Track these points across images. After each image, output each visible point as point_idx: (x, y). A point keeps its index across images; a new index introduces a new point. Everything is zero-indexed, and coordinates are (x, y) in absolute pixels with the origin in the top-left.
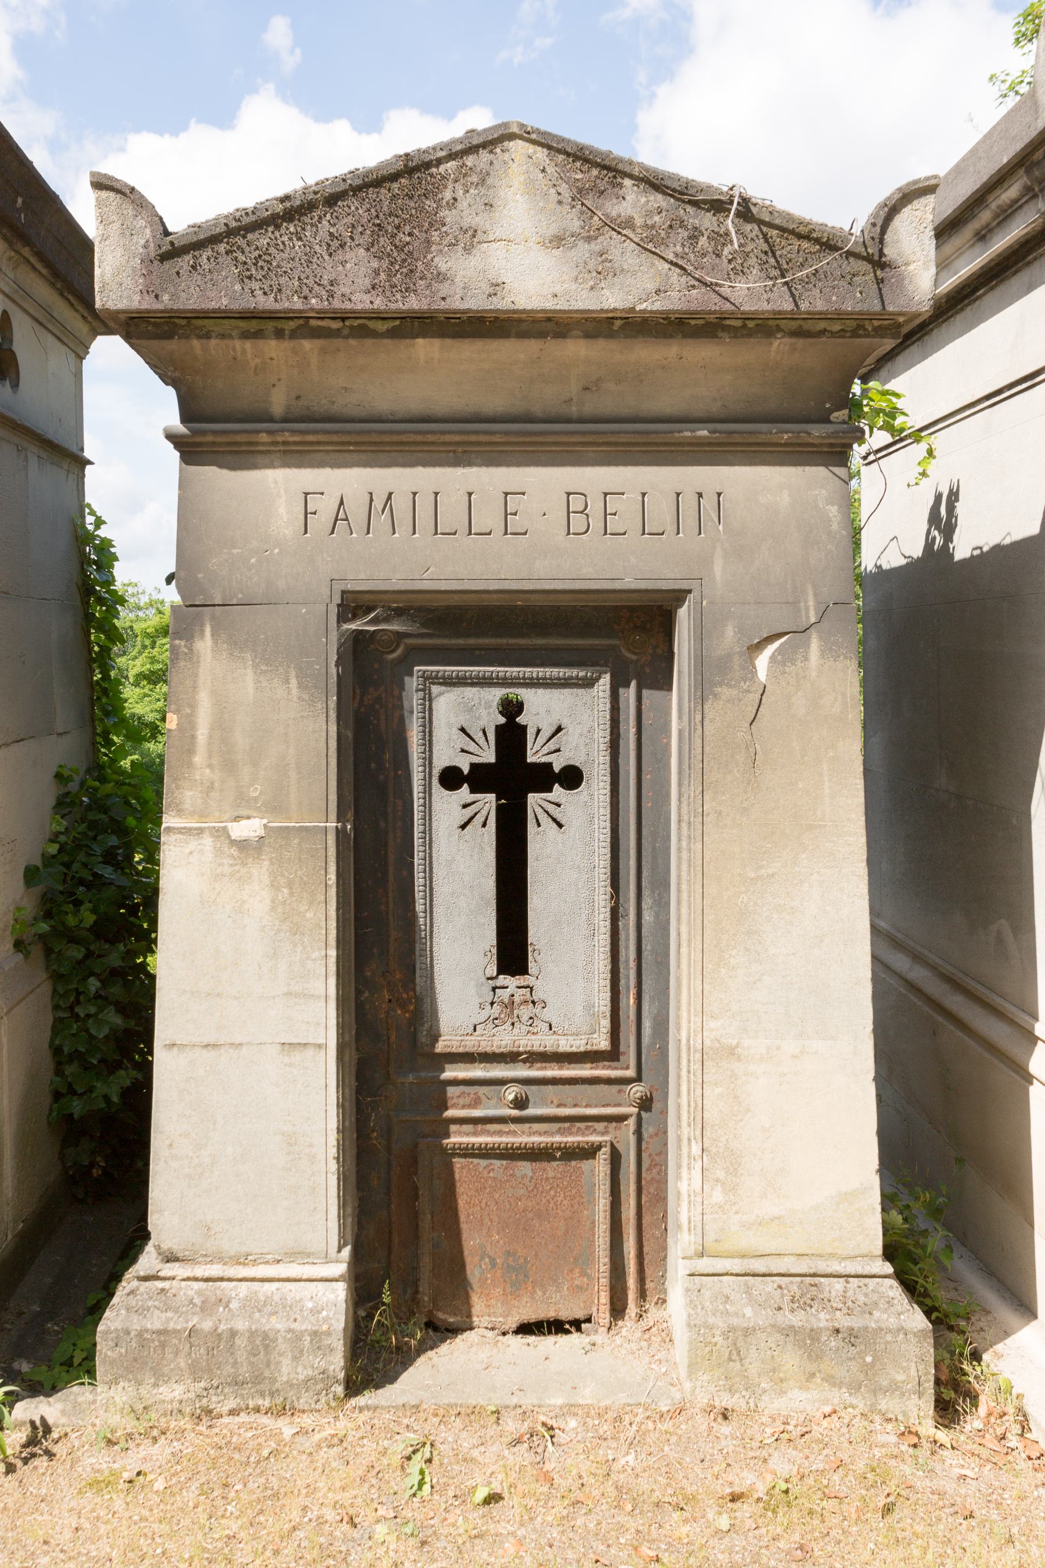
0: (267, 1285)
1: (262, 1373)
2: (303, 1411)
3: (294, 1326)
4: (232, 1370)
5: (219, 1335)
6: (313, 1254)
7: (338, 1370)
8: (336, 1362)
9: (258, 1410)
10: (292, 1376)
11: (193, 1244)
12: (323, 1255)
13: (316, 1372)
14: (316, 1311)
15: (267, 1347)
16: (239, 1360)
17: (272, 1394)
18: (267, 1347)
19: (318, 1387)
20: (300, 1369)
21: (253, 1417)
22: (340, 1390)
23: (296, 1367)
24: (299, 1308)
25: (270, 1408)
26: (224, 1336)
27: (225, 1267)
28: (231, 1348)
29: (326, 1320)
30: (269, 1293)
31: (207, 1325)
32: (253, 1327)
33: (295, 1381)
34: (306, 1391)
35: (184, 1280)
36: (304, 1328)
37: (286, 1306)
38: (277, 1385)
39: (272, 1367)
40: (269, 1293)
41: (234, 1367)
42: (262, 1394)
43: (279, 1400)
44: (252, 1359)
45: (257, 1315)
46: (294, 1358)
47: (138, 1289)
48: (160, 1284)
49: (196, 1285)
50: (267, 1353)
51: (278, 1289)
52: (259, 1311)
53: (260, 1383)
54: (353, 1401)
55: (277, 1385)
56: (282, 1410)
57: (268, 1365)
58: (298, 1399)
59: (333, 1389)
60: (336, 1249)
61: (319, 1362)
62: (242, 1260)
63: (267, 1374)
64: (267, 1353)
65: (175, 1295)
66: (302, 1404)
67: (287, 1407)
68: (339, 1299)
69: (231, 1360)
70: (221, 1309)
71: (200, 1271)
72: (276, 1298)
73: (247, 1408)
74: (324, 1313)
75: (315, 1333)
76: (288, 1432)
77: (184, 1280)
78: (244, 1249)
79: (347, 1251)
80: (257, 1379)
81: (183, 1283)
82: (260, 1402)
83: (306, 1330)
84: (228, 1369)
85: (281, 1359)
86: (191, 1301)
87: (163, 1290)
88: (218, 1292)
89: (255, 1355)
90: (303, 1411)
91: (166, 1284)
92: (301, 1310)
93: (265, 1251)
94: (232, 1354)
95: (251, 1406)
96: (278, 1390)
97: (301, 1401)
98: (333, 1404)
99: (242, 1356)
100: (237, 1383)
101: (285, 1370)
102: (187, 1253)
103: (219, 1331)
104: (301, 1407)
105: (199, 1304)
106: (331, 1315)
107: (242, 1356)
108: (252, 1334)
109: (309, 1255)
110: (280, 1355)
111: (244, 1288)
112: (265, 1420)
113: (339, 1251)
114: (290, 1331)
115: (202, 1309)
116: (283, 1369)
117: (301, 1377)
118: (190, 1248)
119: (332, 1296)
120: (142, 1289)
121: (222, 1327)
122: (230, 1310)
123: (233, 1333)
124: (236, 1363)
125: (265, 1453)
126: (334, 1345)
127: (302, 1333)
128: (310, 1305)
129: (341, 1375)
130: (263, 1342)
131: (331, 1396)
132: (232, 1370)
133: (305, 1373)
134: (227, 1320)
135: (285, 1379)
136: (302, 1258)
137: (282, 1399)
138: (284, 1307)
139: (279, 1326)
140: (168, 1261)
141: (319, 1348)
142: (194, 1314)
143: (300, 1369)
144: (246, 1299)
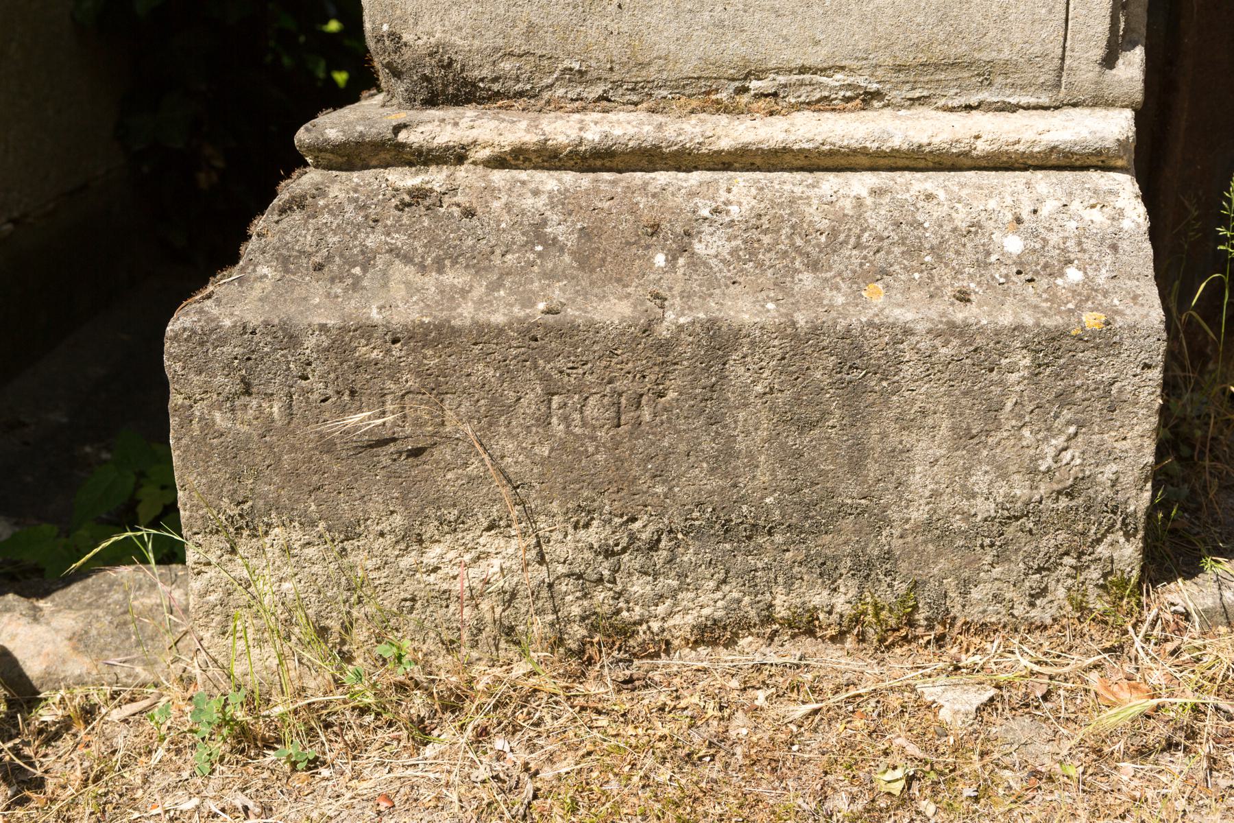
0: (830, 182)
1: (831, 494)
2: (984, 629)
3: (960, 314)
4: (715, 483)
5: (664, 347)
6: (1007, 68)
7: (1127, 480)
8: (1126, 453)
9: (805, 625)
10: (946, 504)
11: (531, 30)
12: (1047, 77)
13: (1043, 489)
14: (1036, 267)
15: (854, 391)
16: (741, 445)
17: (864, 570)
18: (854, 391)
19: (1047, 543)
20: (980, 480)
21: (792, 651)
22: (1127, 553)
23: (968, 472)
24: (969, 255)
25: (856, 620)
26: (686, 349)
27: (658, 118)
28: (711, 400)
29: (1086, 294)
30: (848, 206)
31: (614, 310)
32: (801, 319)
33: (958, 523)
34: (998, 559)
35: (499, 162)
36: (1006, 319)
37: (914, 250)
38: (890, 538)
39: (873, 470)
40: (848, 206)
41: (731, 469)
42: (828, 574)
43: (888, 592)
44: (793, 440)
45: (807, 280)
46: (964, 437)
47: (320, 191)
48: (404, 179)
49: (549, 181)
50: (856, 418)
51: (876, 192)
52: (814, 266)
53: (818, 530)
54: (1181, 594)
55: (890, 538)
56: (900, 628)
57: (856, 466)
58: (965, 586)
59: (1102, 550)
60: (1099, 52)
61: (1058, 451)
62: (723, 96)
63: (849, 494)
64: (856, 418)
65: (469, 213)
66: (979, 603)
67: (920, 617)
68: (1126, 224)
69: (708, 445)
70: (660, 259)
71: (562, 130)
72: (877, 220)
73: (769, 620)
74: (1073, 275)
75: (1055, 337)
76: (956, 702)
77: (499, 162)
78: (735, 49)
79: (1131, 68)
80: (809, 516)
81: (499, 177)
82: (819, 597)
83: (1018, 328)
84: (698, 480)
85: (908, 439)
86: (537, 232)
87: (419, 195)
88: (642, 201)
89: (805, 426)
90: (984, 629)
91: (436, 177)
92: (982, 265)
93: (815, 57)
94: (713, 421)
95: (781, 612)
96: (888, 555)
97: (975, 594)
98: (1099, 605)
99: (752, 427)
100: (731, 529)
101: (919, 479)
102: (507, 66)
103: (663, 332)
104: (974, 614)
105: (571, 241)
106: (1102, 279)
107: (752, 427)
108: (798, 345)
109: (986, 74)
110: (905, 423)
111: (741, 191)
112: (837, 660)
113: (1109, 61)
114: (954, 330)
115: (584, 261)
116: (916, 479)
117: (983, 508)
118: (519, 45)
119: (1098, 217)
120: (335, 191)
121: (673, 318)
122: (695, 262)
123: (719, 342)
124: (728, 453)
125: (891, 780)
126: (1127, 384)
127: (1001, 339)
128: (1014, 245)
129: (1141, 501)
130: (846, 373)
131: (1094, 574)
132: (715, 483)
133: (1001, 491)
134: (686, 296)
135: (918, 514)
136: (962, 89)
137: (901, 588)
138: (913, 251)
139: (905, 315)
140: (431, 102)
141: (1063, 399)
142: (551, 276)
143: (980, 480)
144: (755, 223)
